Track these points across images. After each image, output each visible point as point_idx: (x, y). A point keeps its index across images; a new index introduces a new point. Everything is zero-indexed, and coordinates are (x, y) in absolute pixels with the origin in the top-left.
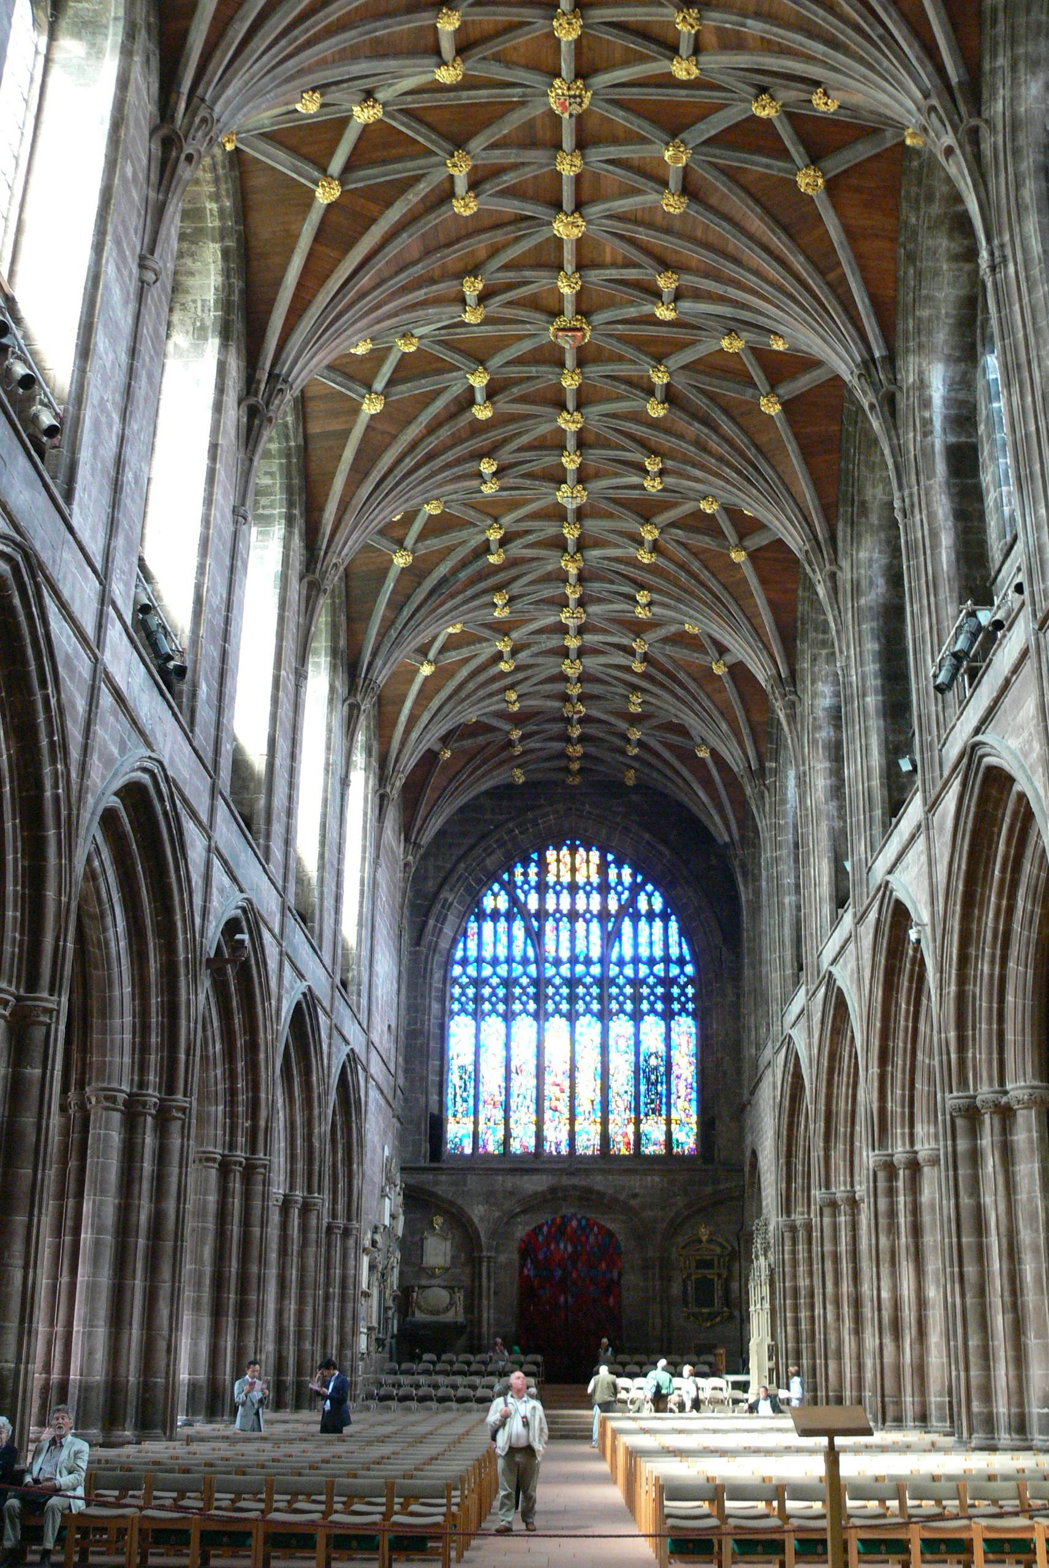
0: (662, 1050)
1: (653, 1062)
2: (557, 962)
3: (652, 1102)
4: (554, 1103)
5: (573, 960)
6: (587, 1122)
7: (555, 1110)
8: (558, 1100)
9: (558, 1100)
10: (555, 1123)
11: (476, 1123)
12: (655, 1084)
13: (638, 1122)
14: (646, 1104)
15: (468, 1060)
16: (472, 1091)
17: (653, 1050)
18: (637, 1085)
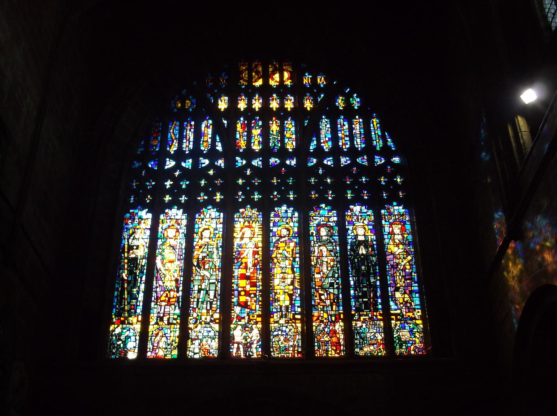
0: (372, 237)
1: (362, 251)
2: (249, 154)
3: (365, 295)
4: (243, 299)
5: (266, 152)
6: (282, 321)
7: (245, 305)
8: (247, 294)
9: (247, 294)
10: (243, 322)
11: (145, 323)
12: (367, 275)
13: (348, 319)
14: (356, 298)
15: (141, 252)
16: (142, 287)
17: (361, 238)
18: (345, 277)
